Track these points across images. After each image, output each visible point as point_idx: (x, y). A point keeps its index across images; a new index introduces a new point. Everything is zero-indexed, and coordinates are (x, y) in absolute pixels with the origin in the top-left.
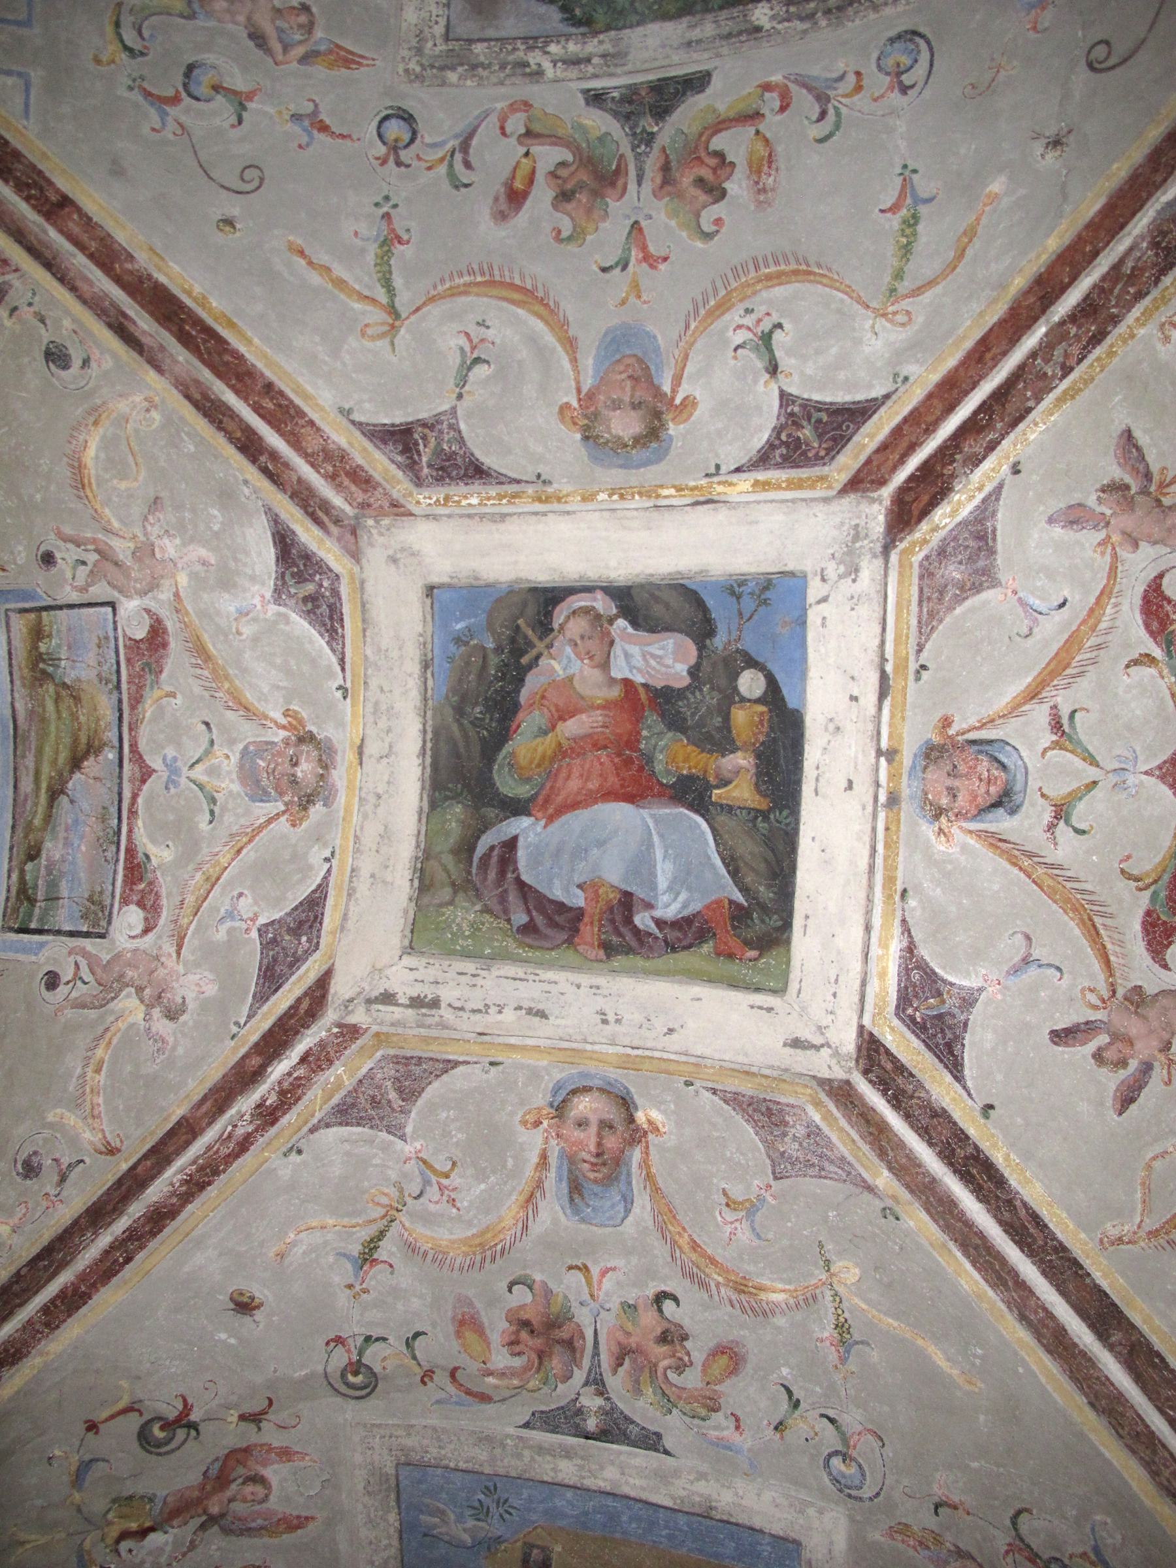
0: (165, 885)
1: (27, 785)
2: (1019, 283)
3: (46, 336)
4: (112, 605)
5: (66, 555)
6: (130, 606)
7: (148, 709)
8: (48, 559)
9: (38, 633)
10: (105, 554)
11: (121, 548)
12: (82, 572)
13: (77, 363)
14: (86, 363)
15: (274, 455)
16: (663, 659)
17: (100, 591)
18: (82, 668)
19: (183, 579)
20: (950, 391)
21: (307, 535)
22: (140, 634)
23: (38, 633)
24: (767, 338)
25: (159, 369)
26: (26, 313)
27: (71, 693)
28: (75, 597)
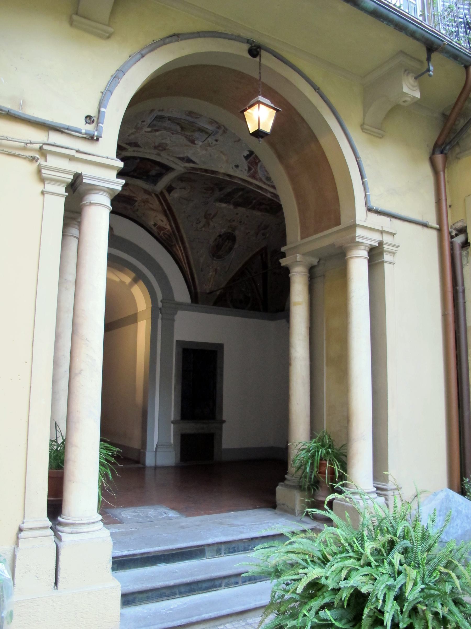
0: (153, 134)
1: (182, 121)
2: (173, 207)
3: (240, 168)
4: (203, 142)
5: (215, 143)
6: (201, 143)
7: (183, 138)
8: (216, 141)
9: (207, 133)
10: (210, 146)
11: (209, 148)
12: (210, 143)
13: (234, 167)
14: (233, 168)
15: (203, 172)
16: (153, 172)
17: (206, 142)
18: (196, 134)
19: (198, 150)
20: (166, 200)
21: (192, 165)
22: (195, 142)
23: (207, 133)
24: (184, 188)
25: (223, 173)
26: (244, 170)
27: (194, 131)
28: (208, 139)
